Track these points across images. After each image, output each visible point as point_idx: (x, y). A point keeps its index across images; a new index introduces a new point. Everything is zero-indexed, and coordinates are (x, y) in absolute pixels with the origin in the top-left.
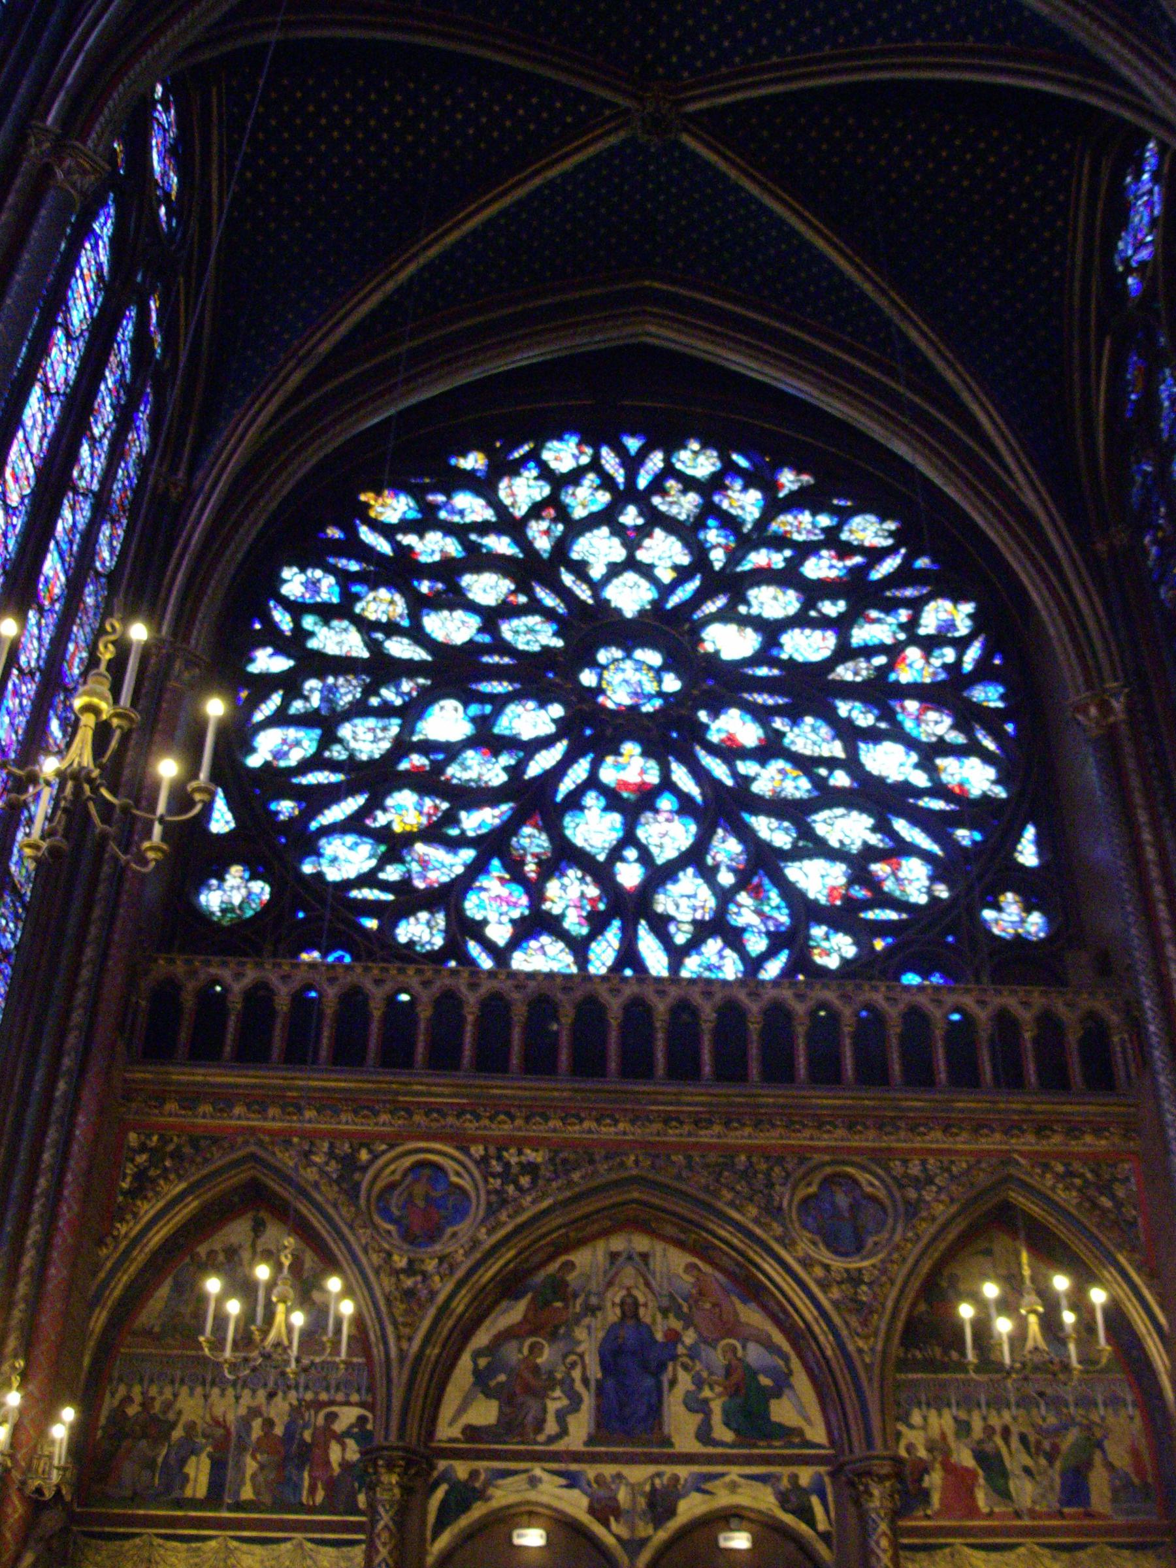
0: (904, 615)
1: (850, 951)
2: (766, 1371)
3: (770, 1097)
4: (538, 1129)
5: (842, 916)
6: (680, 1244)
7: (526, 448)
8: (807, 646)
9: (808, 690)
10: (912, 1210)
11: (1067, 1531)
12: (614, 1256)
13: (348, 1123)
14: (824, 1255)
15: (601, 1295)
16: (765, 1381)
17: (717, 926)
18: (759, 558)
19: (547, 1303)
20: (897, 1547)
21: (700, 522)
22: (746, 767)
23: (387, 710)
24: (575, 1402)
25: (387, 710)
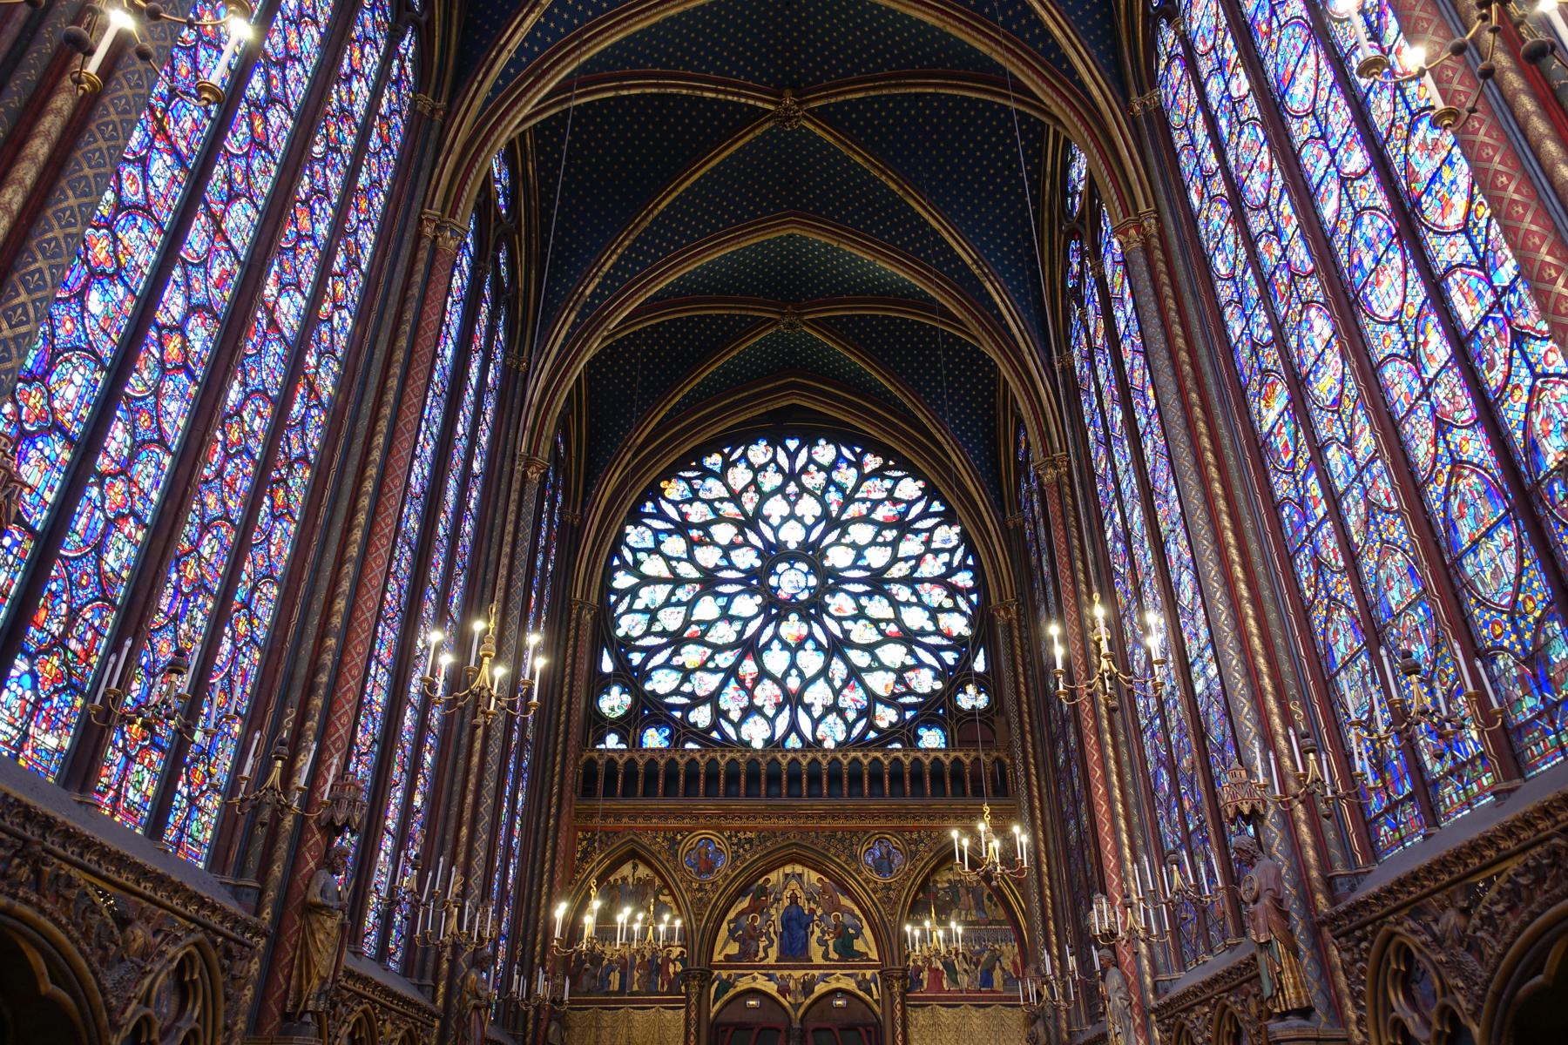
0: (924, 536)
1: (894, 718)
4: (752, 824)
5: (891, 701)
7: (739, 451)
8: (877, 557)
10: (913, 854)
11: (983, 999)
12: (787, 875)
13: (672, 823)
17: (833, 708)
18: (854, 510)
22: (848, 625)
23: (679, 603)
24: (771, 942)
25: (679, 603)
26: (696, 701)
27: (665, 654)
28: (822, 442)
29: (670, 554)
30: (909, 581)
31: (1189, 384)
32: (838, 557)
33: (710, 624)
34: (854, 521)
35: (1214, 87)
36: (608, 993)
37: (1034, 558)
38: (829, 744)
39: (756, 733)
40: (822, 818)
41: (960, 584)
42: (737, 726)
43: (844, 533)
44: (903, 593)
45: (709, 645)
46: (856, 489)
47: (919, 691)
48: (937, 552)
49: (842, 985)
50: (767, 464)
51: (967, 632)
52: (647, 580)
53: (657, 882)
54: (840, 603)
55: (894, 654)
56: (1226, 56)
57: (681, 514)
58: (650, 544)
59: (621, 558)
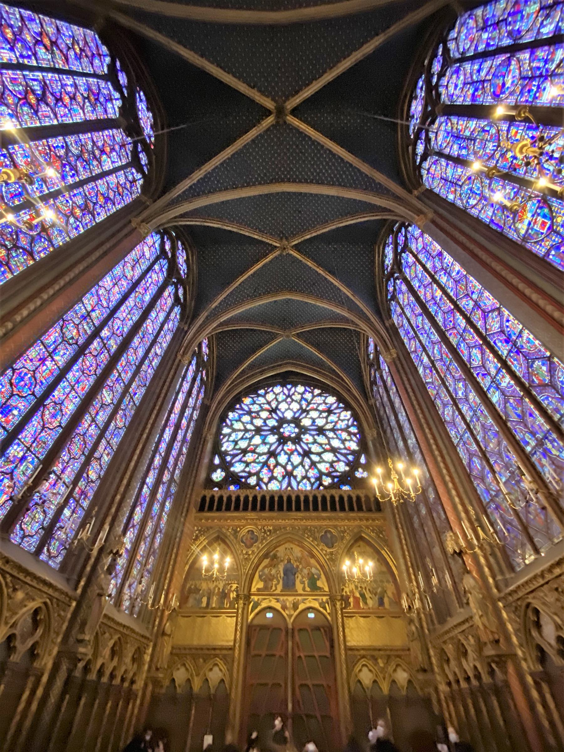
2: (316, 574)
3: (314, 514)
4: (270, 522)
5: (328, 475)
6: (299, 546)
7: (271, 389)
8: (320, 422)
9: (321, 431)
10: (343, 538)
14: (326, 548)
16: (316, 576)
17: (306, 477)
21: (301, 400)
24: (279, 582)
25: (246, 438)
26: (250, 474)
32: (306, 422)
33: (257, 446)
36: (201, 608)
40: (301, 520)
42: (266, 484)
43: (308, 414)
45: (256, 453)
52: (234, 430)
55: (329, 457)
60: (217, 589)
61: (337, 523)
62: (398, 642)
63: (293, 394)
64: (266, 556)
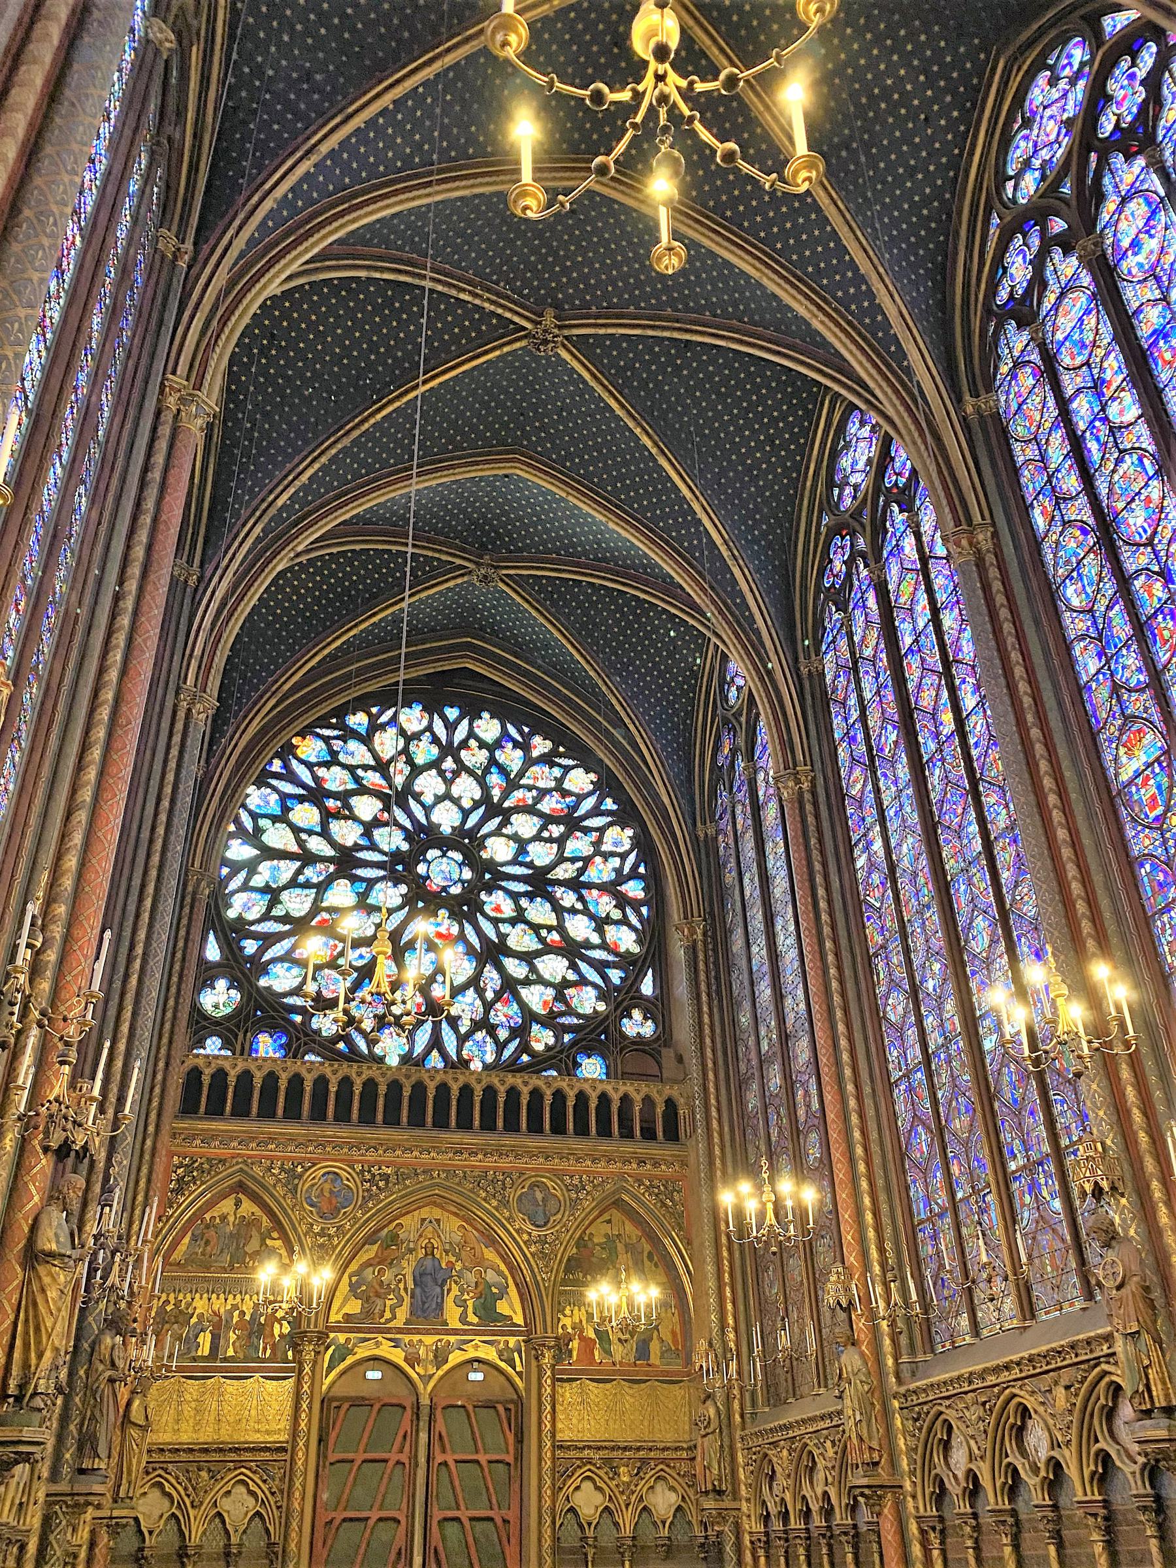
4: (389, 1157)
5: (549, 1021)
7: (390, 713)
8: (541, 854)
9: (540, 883)
12: (423, 1220)
13: (293, 1152)
14: (529, 1227)
15: (416, 1242)
16: (494, 1290)
17: (483, 1024)
19: (388, 1246)
20: (555, 1380)
21: (487, 771)
22: (505, 928)
23: (307, 885)
25: (307, 885)
26: (324, 1004)
27: (286, 944)
28: (486, 715)
29: (301, 825)
30: (575, 885)
31: (1030, 718)
32: (499, 850)
34: (517, 810)
35: (1082, 407)
37: (730, 878)
38: (476, 1065)
39: (391, 1047)
41: (630, 894)
43: (506, 822)
44: (568, 899)
46: (521, 774)
47: (580, 1011)
48: (606, 856)
49: (480, 1354)
50: (423, 732)
51: (636, 949)
53: (266, 1222)
54: (498, 902)
55: (554, 967)
56: (1108, 375)
57: (315, 778)
58: (277, 811)
59: (237, 821)
60: (236, 1313)
61: (564, 1165)
62: (667, 1435)
63: (464, 744)
64: (370, 1240)
